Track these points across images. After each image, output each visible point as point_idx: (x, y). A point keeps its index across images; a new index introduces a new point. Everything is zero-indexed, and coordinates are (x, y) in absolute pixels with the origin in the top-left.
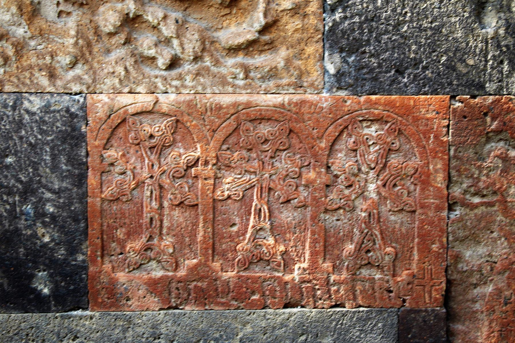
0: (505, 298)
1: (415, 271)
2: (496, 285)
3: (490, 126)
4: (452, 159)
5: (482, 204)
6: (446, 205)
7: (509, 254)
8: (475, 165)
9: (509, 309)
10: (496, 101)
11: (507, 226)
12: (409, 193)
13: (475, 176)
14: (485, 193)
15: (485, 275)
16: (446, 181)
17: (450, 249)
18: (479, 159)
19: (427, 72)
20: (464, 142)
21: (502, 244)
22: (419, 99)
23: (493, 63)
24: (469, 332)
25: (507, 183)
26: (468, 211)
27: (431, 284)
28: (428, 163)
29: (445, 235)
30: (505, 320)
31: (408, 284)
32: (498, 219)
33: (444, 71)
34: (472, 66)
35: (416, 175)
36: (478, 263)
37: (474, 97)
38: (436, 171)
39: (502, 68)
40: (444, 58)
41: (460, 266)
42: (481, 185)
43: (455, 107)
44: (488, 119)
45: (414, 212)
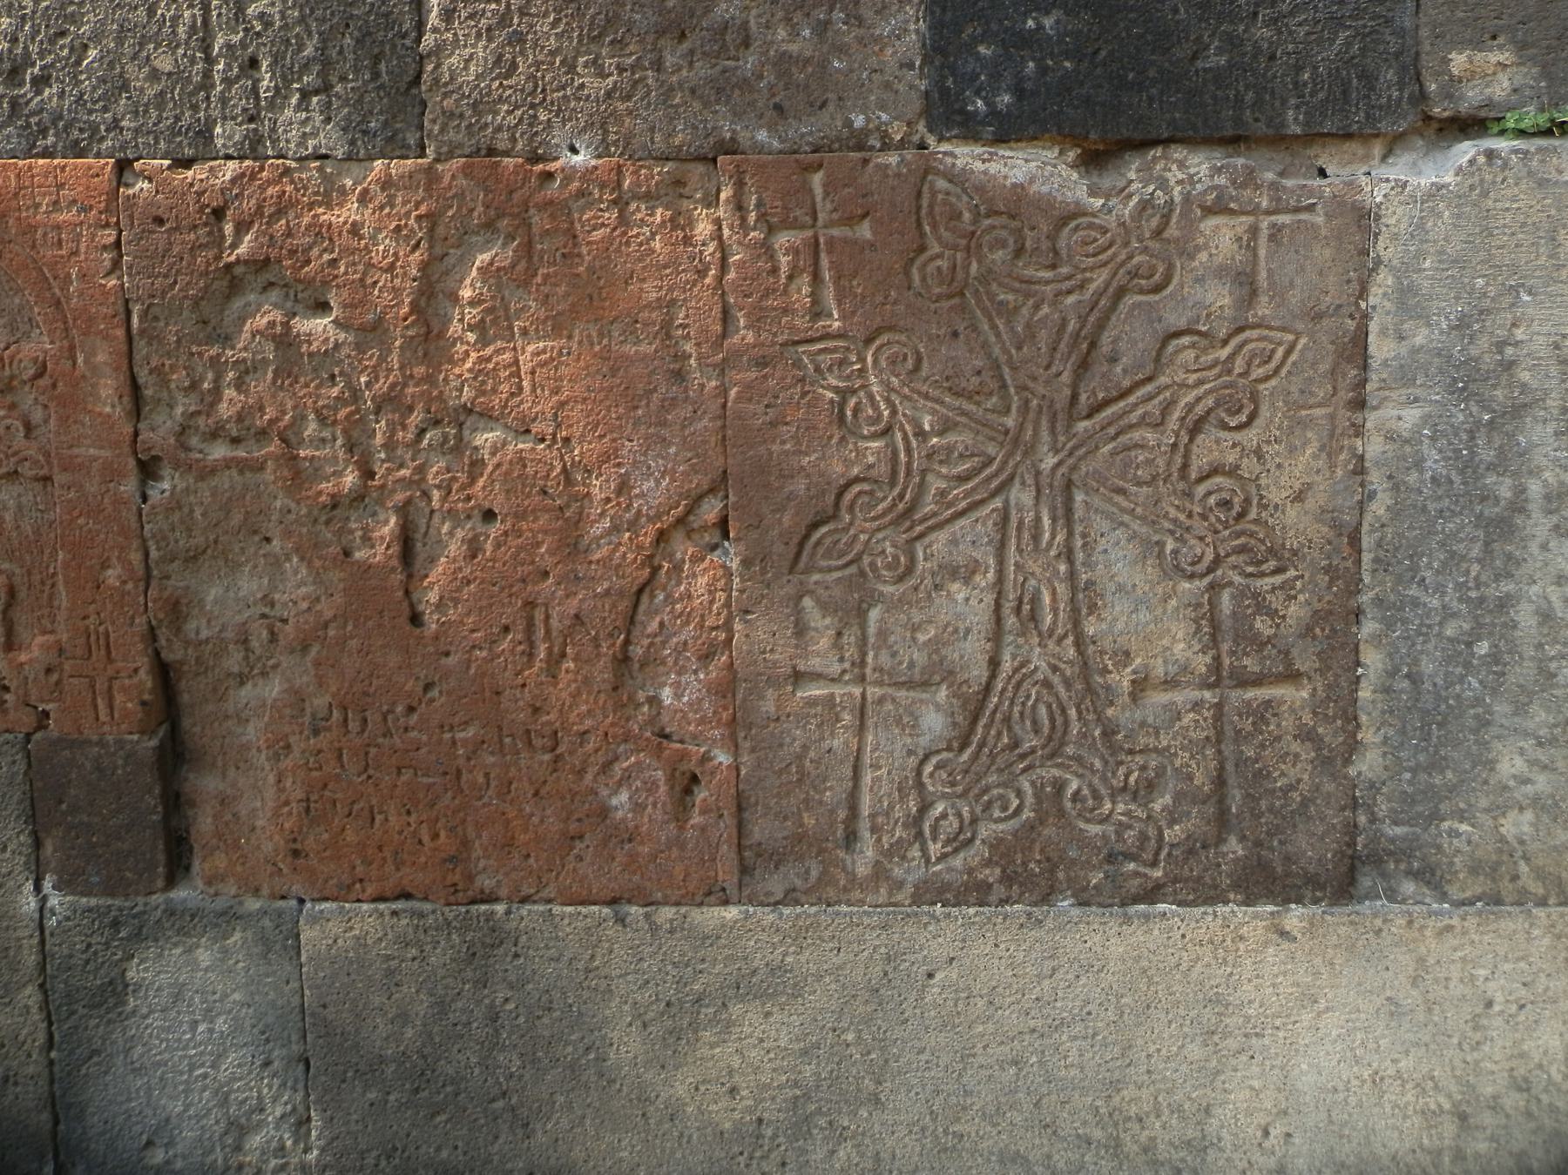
0: (313, 716)
1: (65, 637)
2: (288, 680)
3: (234, 246)
4: (136, 338)
5: (228, 464)
6: (132, 463)
7: (318, 599)
8: (200, 354)
9: (324, 746)
10: (243, 175)
11: (303, 525)
12: (29, 428)
13: (206, 385)
14: (234, 433)
15: (258, 652)
16: (126, 399)
17: (154, 583)
18: (209, 341)
19: (47, 92)
20: (164, 293)
21: (296, 573)
22: (30, 168)
23: (229, 66)
24: (235, 798)
25: (295, 407)
26: (191, 480)
27: (110, 672)
28: (72, 348)
29: (135, 544)
30: (315, 774)
31: (49, 671)
32: (278, 504)
33: (94, 89)
34: (170, 74)
35: (42, 382)
36: (239, 619)
37: (187, 163)
38: (94, 369)
39: (258, 80)
40: (93, 53)
41: (191, 626)
42: (225, 410)
43: (131, 192)
44: (228, 228)
45: (47, 479)
